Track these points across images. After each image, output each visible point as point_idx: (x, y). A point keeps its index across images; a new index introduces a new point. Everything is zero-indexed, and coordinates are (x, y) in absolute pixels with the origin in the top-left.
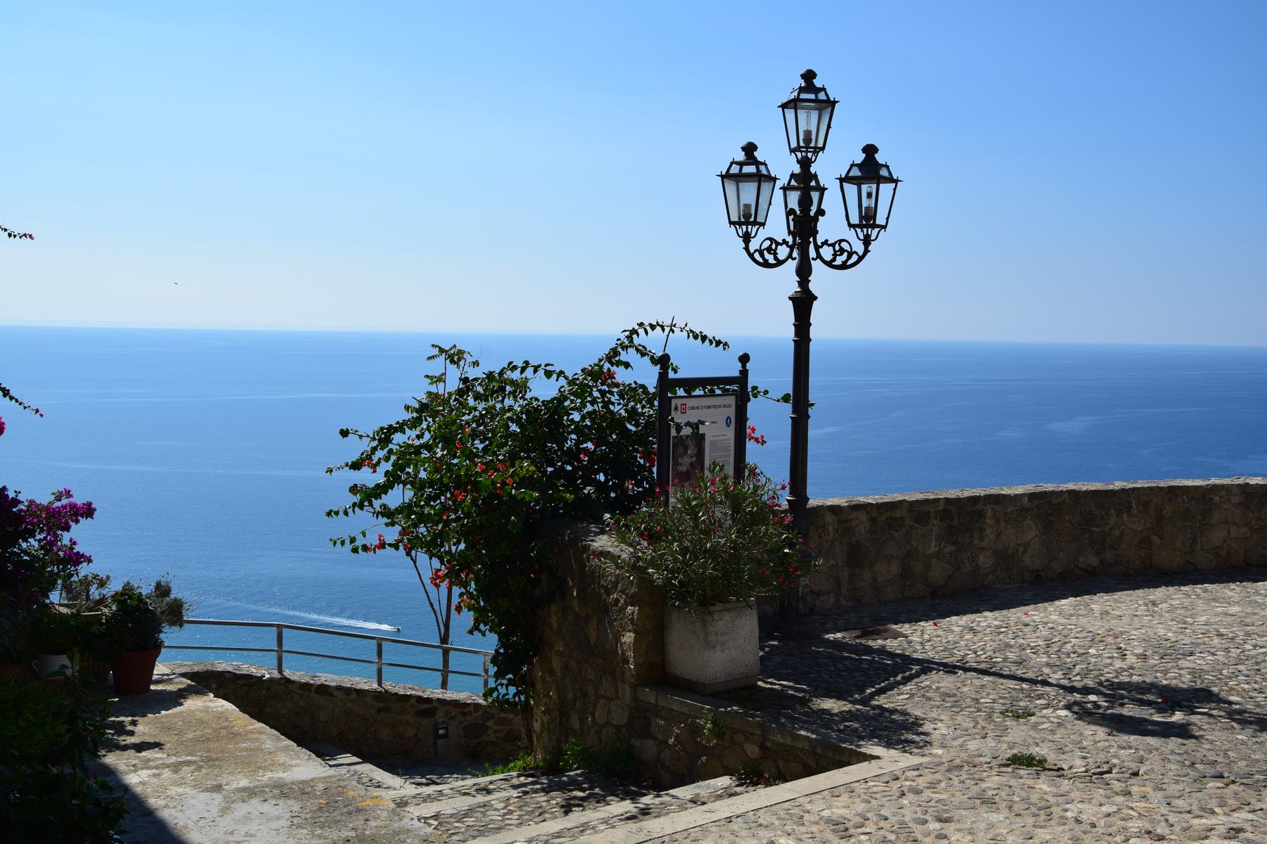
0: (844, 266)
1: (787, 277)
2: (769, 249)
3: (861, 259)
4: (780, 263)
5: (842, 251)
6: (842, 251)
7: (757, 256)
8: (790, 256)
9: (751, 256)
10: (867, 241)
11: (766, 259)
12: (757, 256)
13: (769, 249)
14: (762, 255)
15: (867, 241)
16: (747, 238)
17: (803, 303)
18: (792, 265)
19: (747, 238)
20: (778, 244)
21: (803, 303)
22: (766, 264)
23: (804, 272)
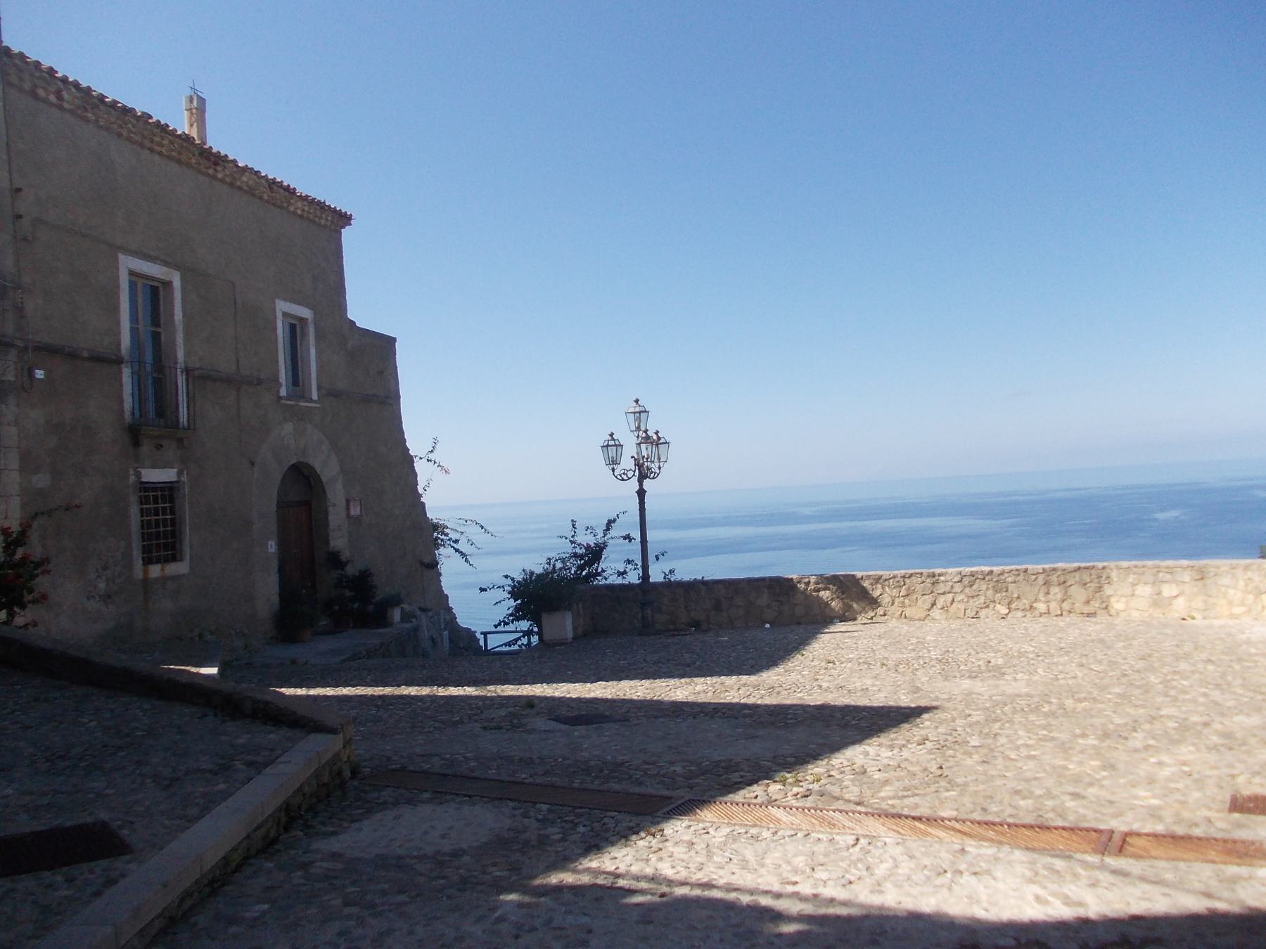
0: (653, 478)
1: (634, 484)
2: (624, 474)
3: (658, 475)
4: (629, 478)
5: (652, 472)
6: (652, 472)
7: (619, 477)
8: (634, 475)
9: (616, 477)
10: (660, 468)
11: (623, 478)
12: (619, 477)
13: (624, 474)
14: (621, 476)
15: (660, 468)
16: (613, 470)
17: (641, 493)
18: (635, 479)
19: (613, 470)
20: (627, 471)
21: (641, 493)
22: (623, 480)
23: (640, 482)
